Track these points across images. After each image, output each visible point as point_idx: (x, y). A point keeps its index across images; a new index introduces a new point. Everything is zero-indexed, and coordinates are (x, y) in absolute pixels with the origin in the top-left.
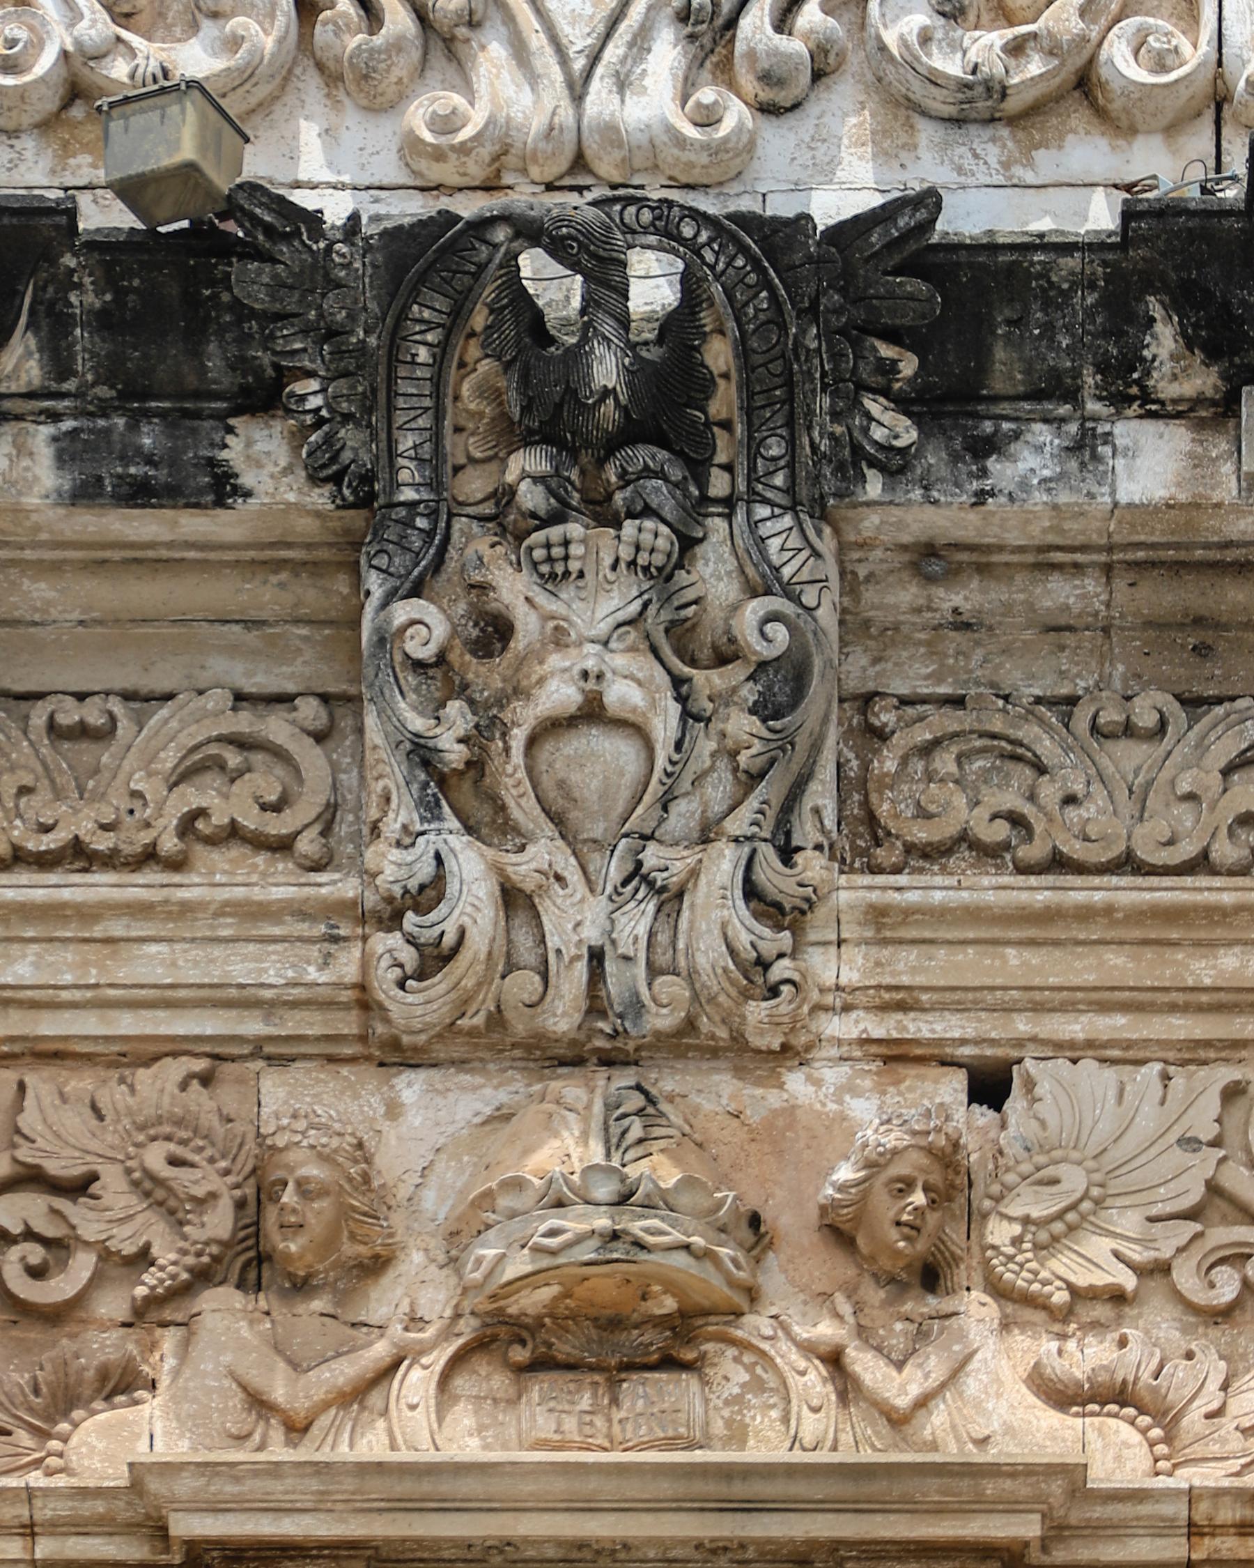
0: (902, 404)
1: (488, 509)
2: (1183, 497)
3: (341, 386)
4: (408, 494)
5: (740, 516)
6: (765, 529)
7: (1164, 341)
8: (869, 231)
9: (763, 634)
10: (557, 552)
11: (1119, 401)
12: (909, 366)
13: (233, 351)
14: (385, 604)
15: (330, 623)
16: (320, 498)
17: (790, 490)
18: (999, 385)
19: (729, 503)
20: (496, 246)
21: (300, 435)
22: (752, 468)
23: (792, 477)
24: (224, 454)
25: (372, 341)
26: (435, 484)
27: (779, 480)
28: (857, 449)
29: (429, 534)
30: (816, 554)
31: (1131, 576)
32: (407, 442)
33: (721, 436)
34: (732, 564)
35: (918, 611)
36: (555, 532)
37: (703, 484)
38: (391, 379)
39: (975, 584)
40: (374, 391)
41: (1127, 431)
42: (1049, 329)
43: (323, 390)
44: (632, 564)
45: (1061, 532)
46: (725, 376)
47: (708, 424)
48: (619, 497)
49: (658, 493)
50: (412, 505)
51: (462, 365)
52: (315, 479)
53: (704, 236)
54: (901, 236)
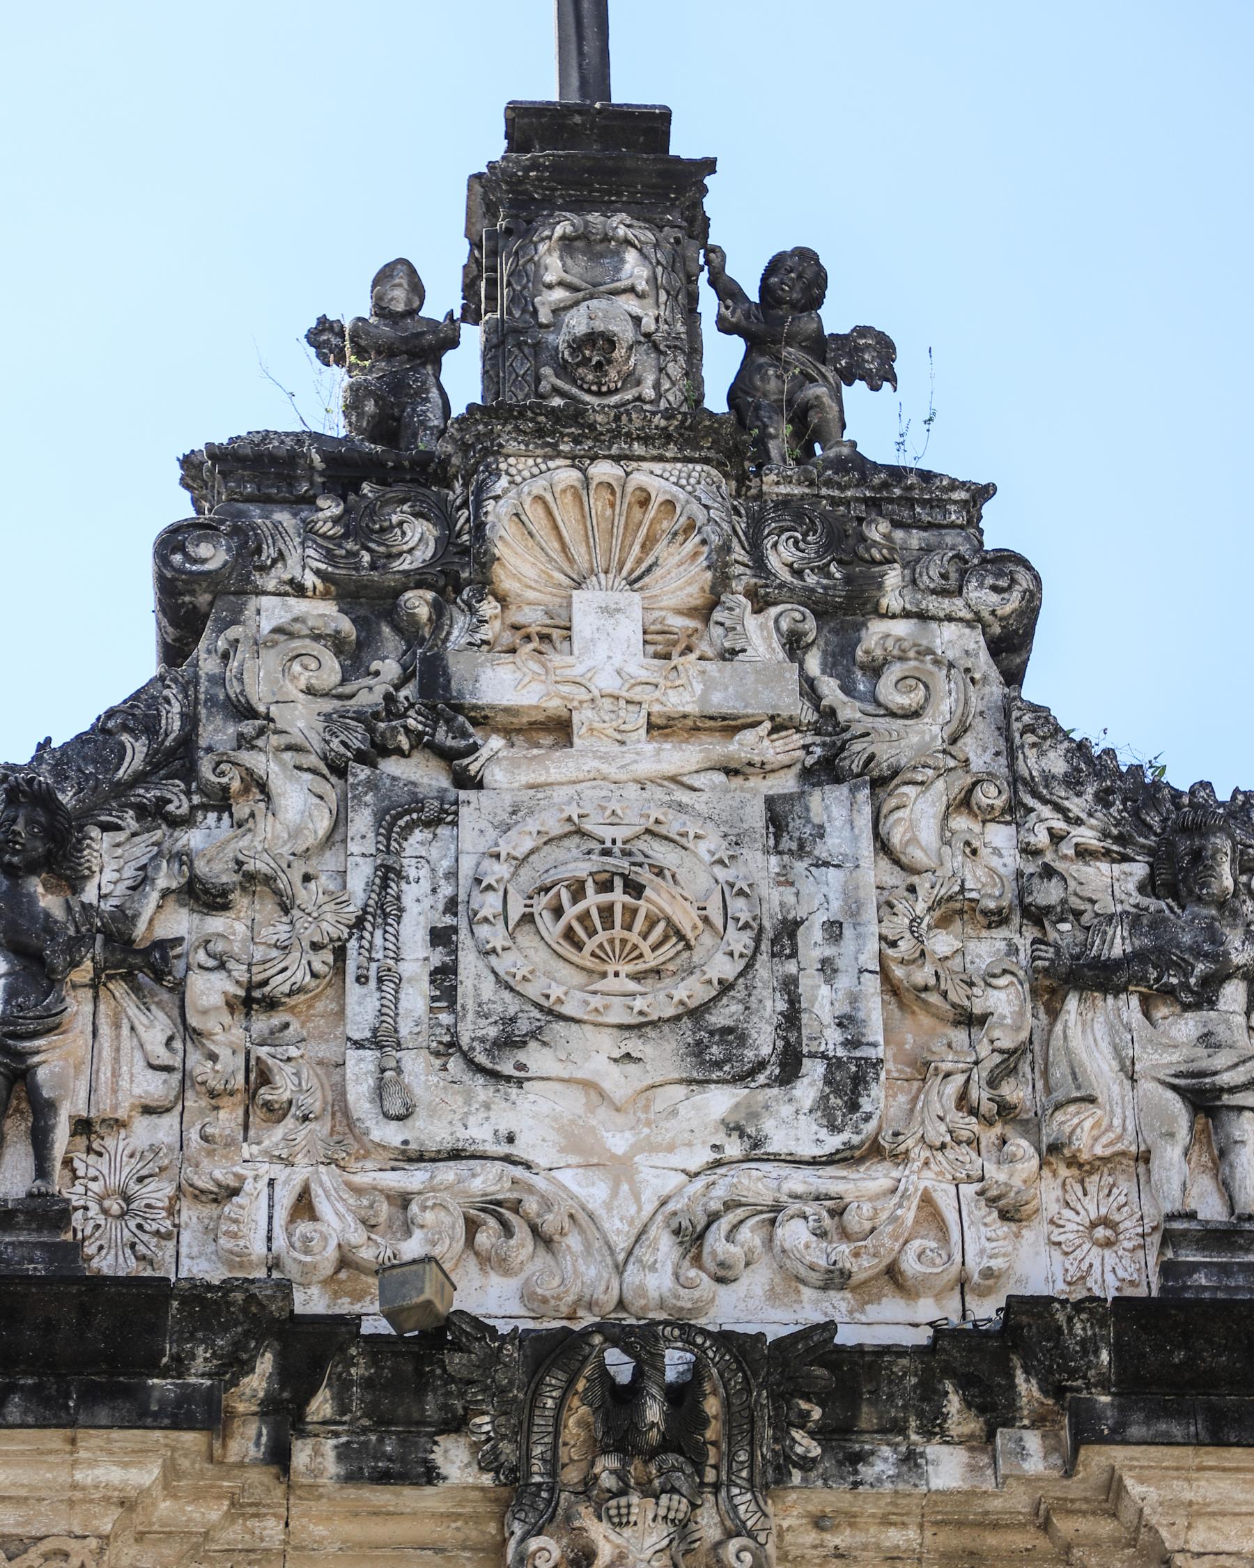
0: (812, 1434)
1: (581, 1489)
2: (966, 1487)
3: (502, 1420)
4: (537, 1479)
5: (723, 1493)
6: (737, 1501)
7: (954, 1404)
8: (797, 1343)
9: (738, 1558)
10: (624, 1511)
11: (928, 1434)
12: (817, 1413)
13: (441, 1400)
14: (523, 1540)
15: (482, 1550)
16: (487, 1479)
17: (750, 1479)
18: (863, 1425)
19: (716, 1487)
20: (593, 1346)
21: (475, 1447)
22: (730, 1467)
23: (751, 1473)
24: (432, 1456)
25: (521, 1396)
26: (553, 1473)
27: (744, 1474)
28: (787, 1458)
29: (549, 1501)
30: (765, 1515)
31: (934, 1530)
32: (537, 1451)
33: (712, 1451)
34: (717, 1519)
35: (815, 1547)
36: (623, 1501)
37: (701, 1474)
38: (531, 1416)
39: (848, 1532)
40: (521, 1423)
41: (934, 1450)
42: (891, 1396)
43: (492, 1422)
44: (665, 1518)
45: (896, 1505)
46: (715, 1417)
47: (705, 1443)
48: (656, 1483)
49: (679, 1480)
50: (539, 1485)
51: (570, 1409)
52: (482, 1469)
53: (708, 1343)
54: (815, 1342)
